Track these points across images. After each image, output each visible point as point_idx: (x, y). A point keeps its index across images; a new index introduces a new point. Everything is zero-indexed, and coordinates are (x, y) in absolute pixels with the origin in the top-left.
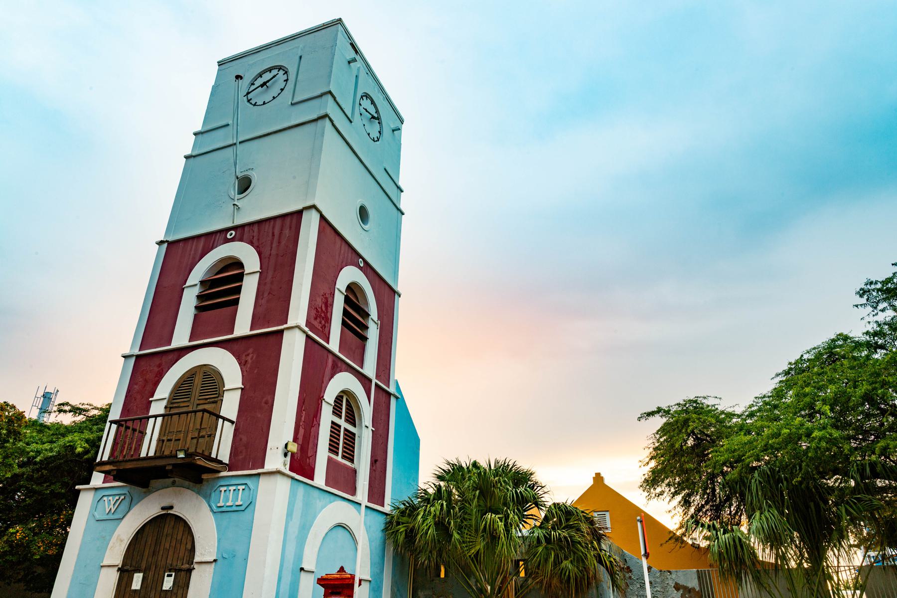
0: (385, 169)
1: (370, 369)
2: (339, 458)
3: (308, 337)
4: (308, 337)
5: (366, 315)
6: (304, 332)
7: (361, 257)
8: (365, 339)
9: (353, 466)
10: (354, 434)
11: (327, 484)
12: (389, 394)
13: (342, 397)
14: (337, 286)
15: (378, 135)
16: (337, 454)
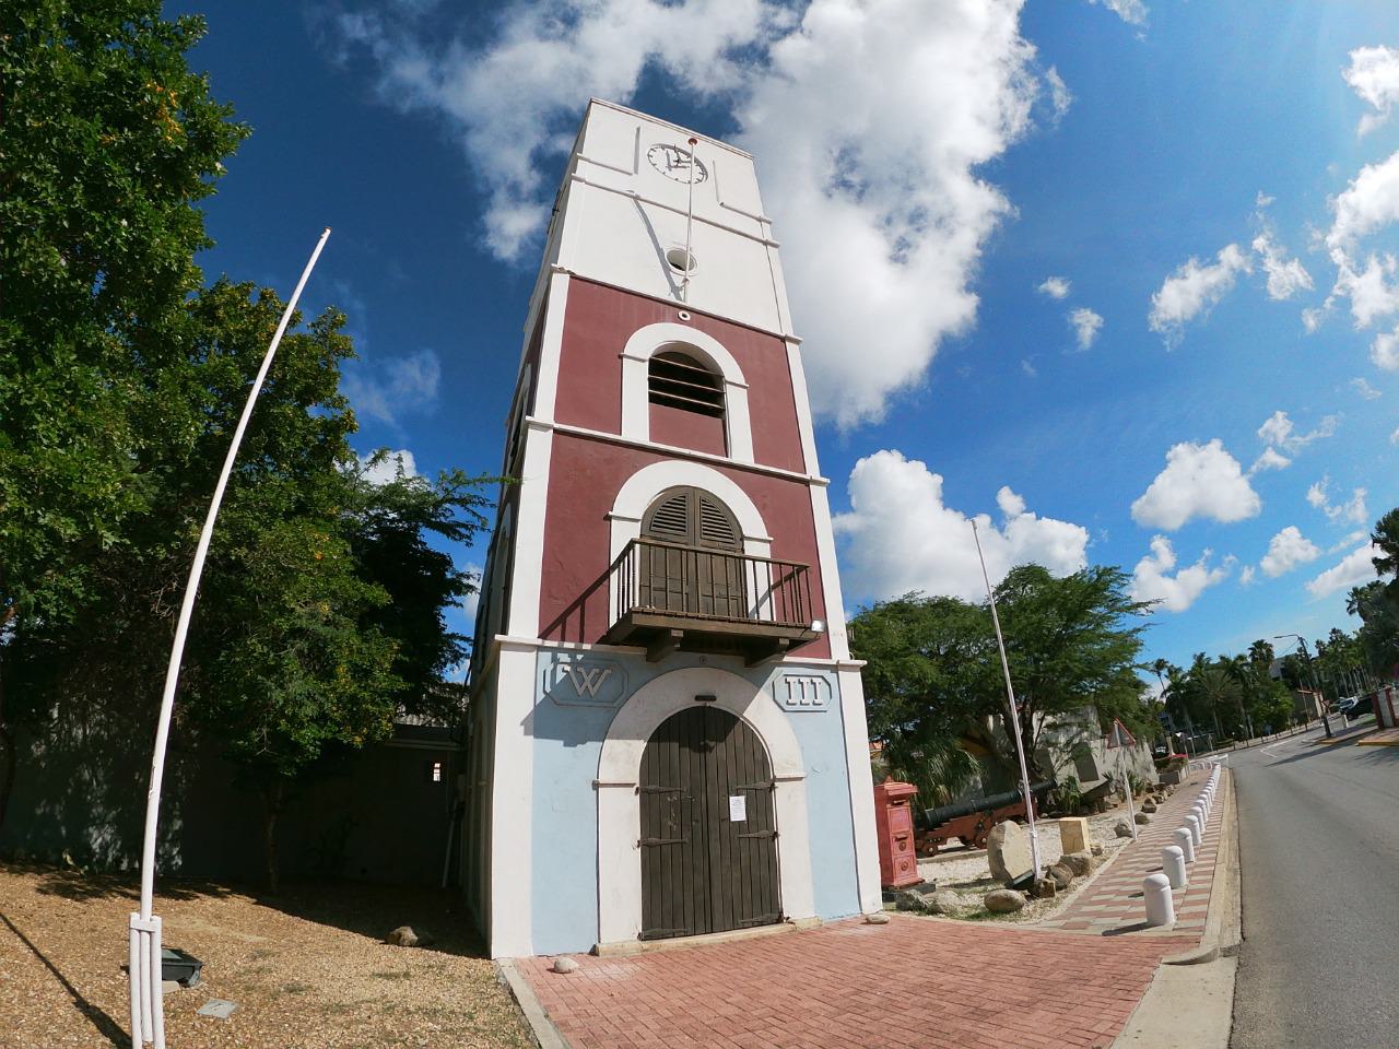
1: (742, 450)
8: (719, 413)
12: (807, 483)
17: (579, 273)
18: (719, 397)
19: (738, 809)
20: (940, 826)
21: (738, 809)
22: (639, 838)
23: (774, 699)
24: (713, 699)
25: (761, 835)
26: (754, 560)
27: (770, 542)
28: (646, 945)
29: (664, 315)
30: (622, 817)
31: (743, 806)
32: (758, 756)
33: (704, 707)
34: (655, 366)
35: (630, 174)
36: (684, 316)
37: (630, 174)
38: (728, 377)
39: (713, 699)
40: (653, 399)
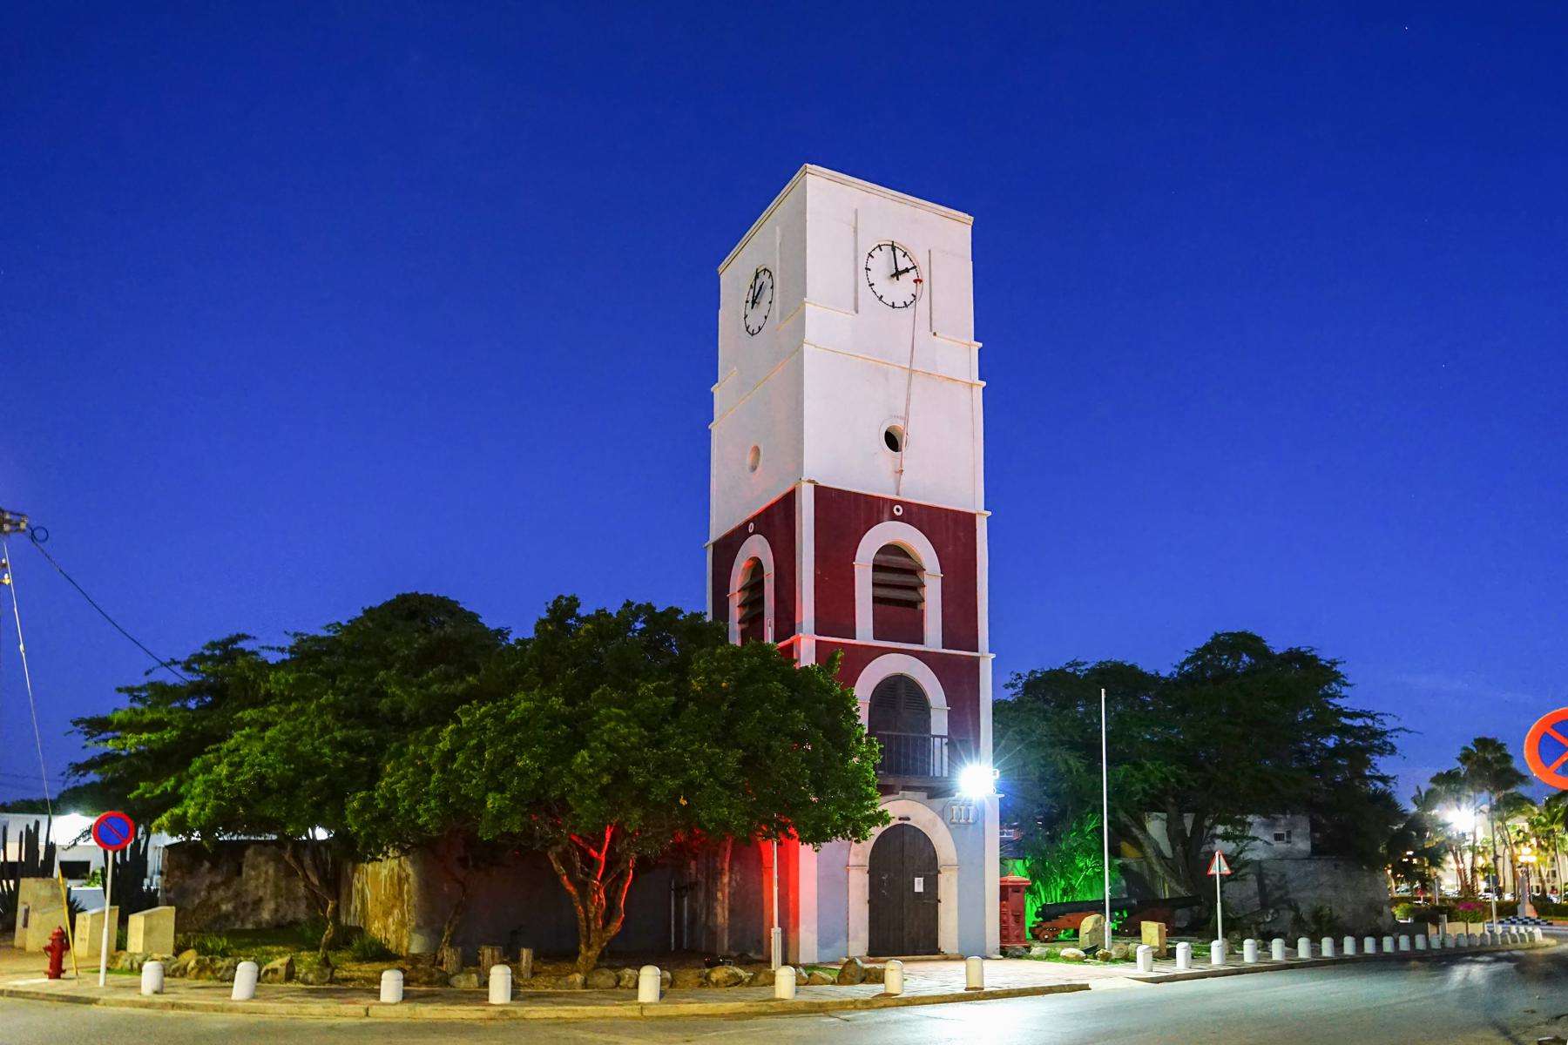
12: (978, 658)
17: (821, 484)
18: (918, 587)
19: (919, 886)
20: (1057, 918)
21: (919, 886)
22: (868, 898)
23: (943, 819)
24: (908, 819)
25: (931, 900)
26: (942, 737)
28: (872, 959)
29: (883, 513)
30: (858, 885)
31: (922, 884)
32: (932, 854)
33: (903, 825)
34: (877, 568)
36: (898, 510)
39: (908, 819)
40: (876, 600)
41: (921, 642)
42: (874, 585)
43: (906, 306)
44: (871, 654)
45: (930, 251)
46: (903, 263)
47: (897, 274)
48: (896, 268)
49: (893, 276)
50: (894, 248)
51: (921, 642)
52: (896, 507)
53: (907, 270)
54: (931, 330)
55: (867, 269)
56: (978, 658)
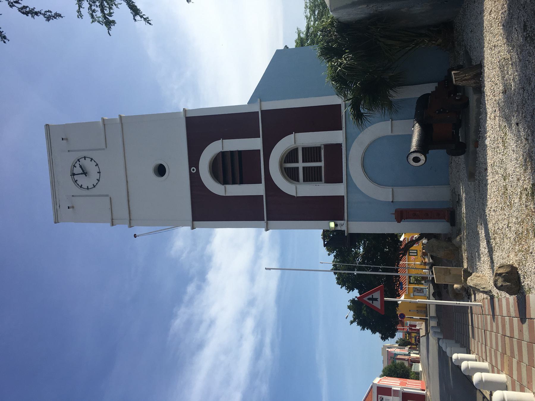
0: (106, 148)
2: (322, 164)
3: (268, 219)
4: (268, 220)
5: (223, 154)
6: (267, 224)
7: (191, 173)
8: (240, 152)
9: (323, 147)
10: (303, 149)
11: (341, 181)
12: (262, 111)
13: (285, 168)
14: (225, 195)
15: (88, 160)
16: (320, 167)
18: (232, 152)
27: (295, 133)
34: (225, 182)
35: (110, 198)
36: (193, 170)
37: (110, 198)
38: (219, 150)
40: (241, 182)
41: (260, 150)
42: (234, 183)
43: (97, 165)
44: (270, 185)
45: (69, 151)
46: (78, 170)
47: (85, 173)
48: (82, 174)
49: (86, 176)
50: (74, 174)
51: (260, 150)
52: (192, 171)
53: (81, 167)
54: (104, 149)
55: (88, 188)
56: (262, 111)
